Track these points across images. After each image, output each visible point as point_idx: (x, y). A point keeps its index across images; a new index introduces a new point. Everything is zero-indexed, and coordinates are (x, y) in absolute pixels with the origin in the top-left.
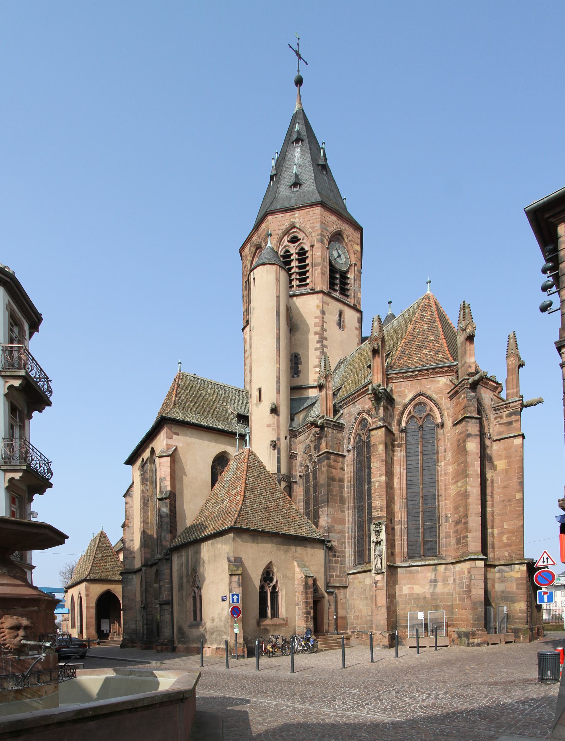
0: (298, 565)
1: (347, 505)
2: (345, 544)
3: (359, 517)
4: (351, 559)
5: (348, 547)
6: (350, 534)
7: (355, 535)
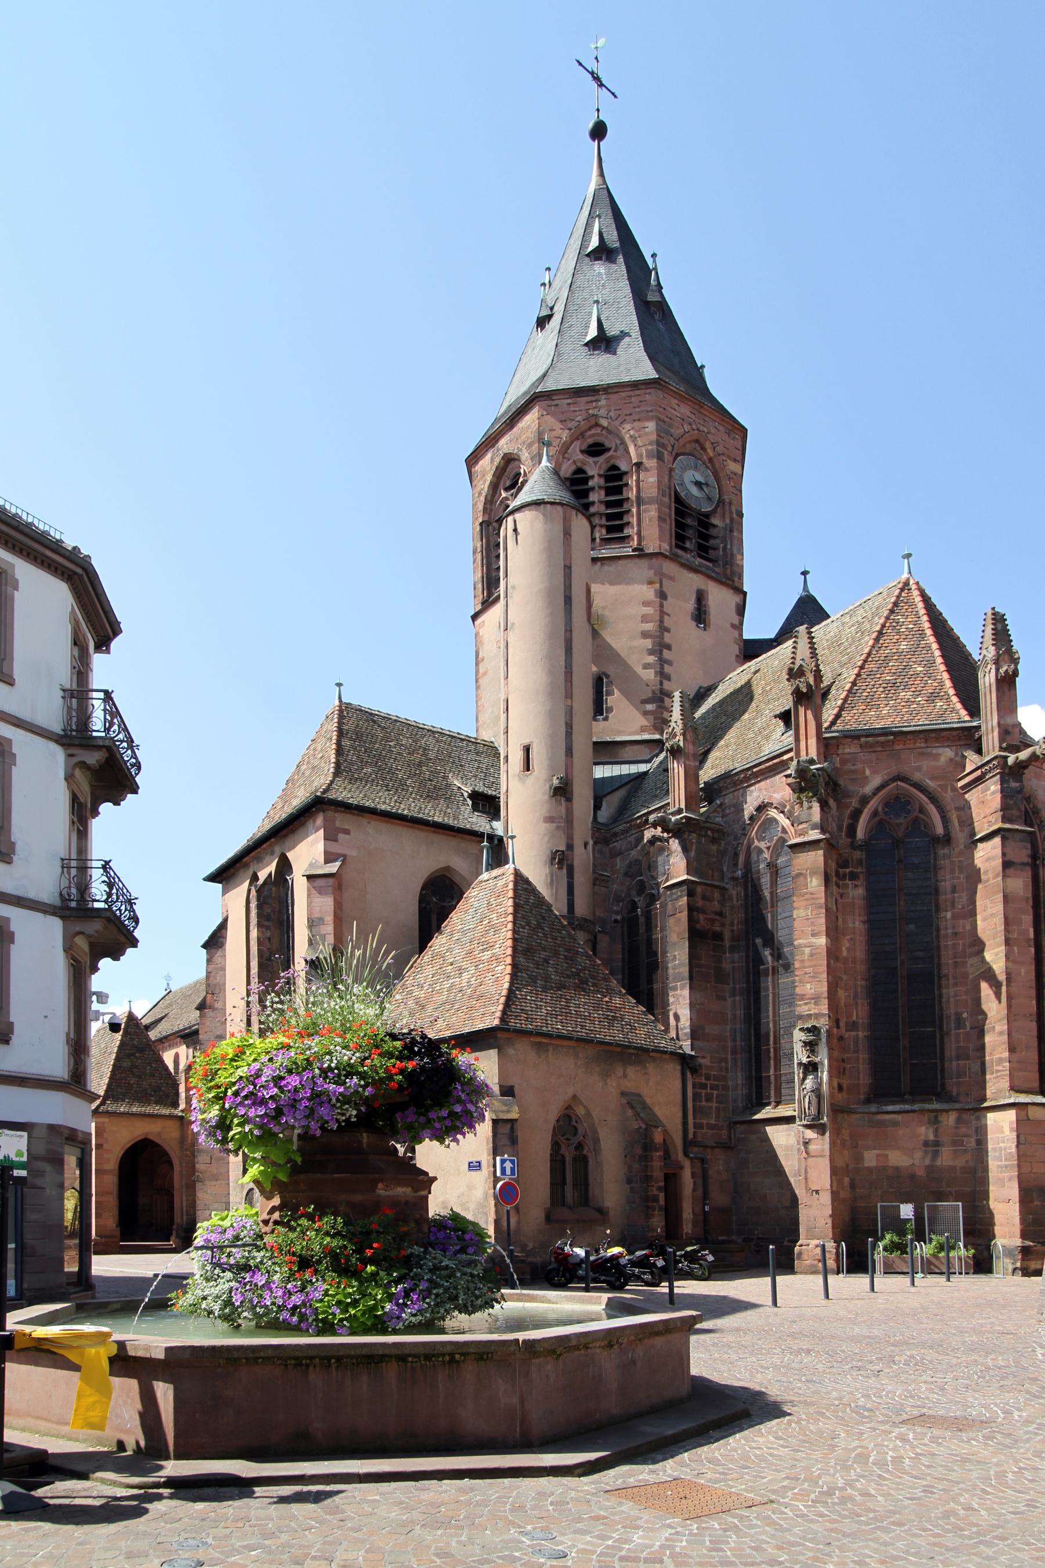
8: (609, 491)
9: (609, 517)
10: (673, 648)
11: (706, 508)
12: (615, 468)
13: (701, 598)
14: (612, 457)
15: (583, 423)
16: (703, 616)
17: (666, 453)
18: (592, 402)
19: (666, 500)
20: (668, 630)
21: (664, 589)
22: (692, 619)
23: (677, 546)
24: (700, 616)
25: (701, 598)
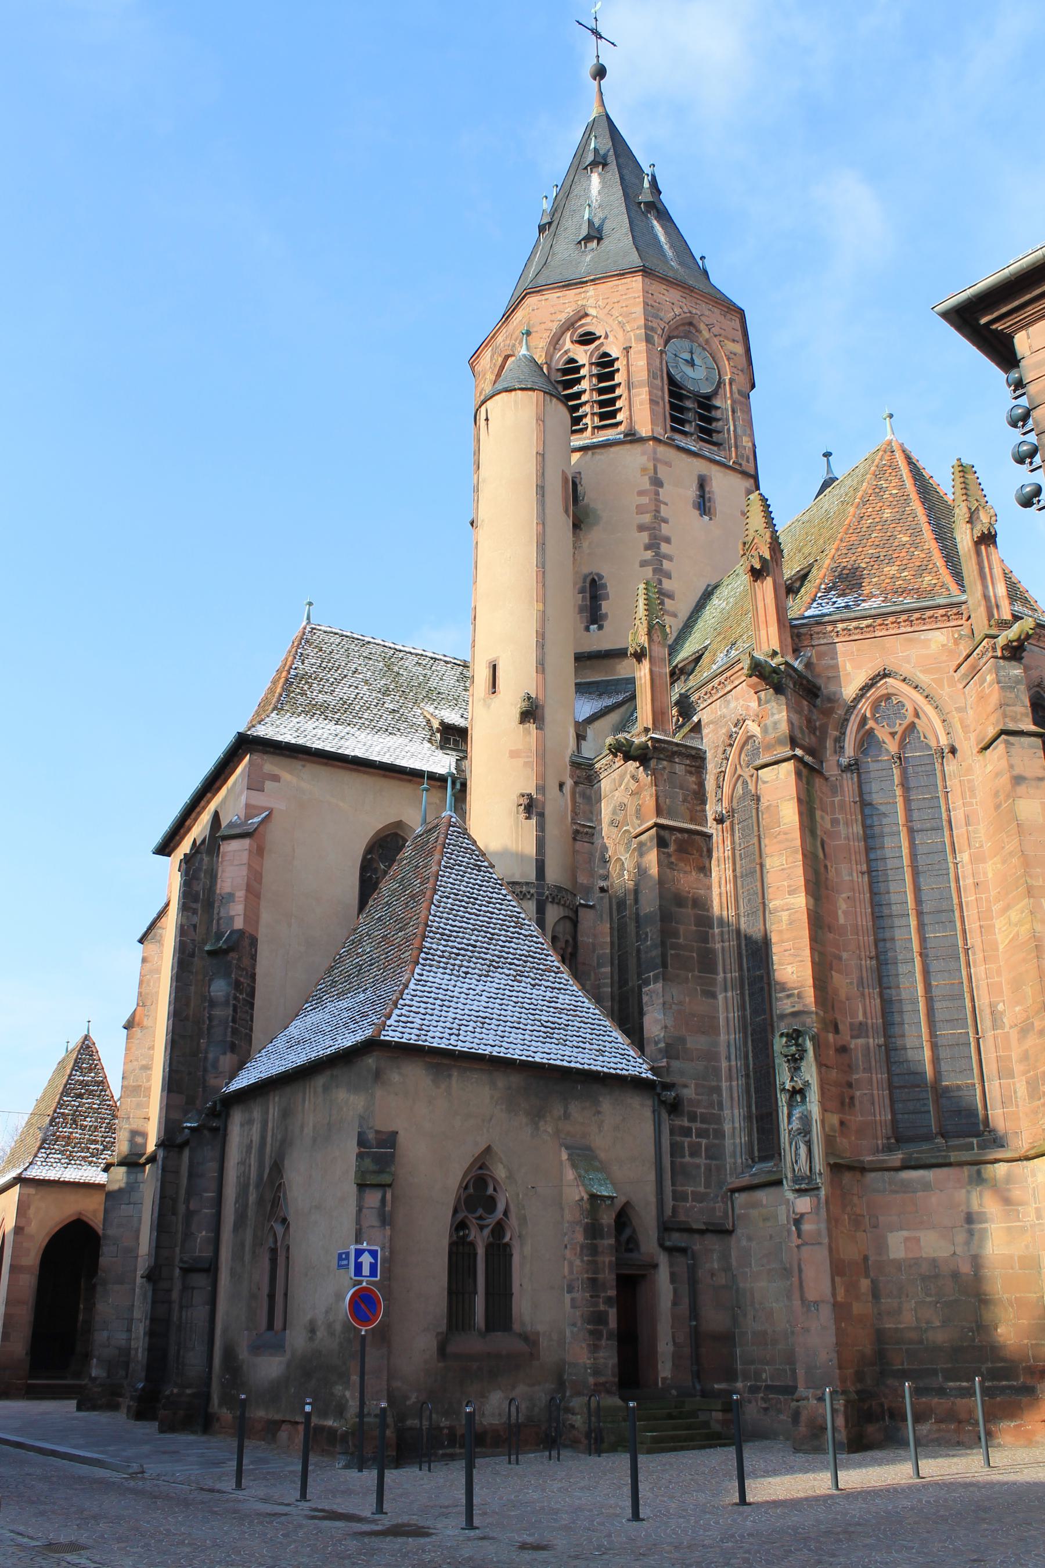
0: (570, 1158)
1: (721, 975)
2: (720, 1095)
3: (755, 1012)
4: (738, 1141)
5: (729, 1103)
6: (733, 1063)
7: (747, 1066)
8: (601, 378)
9: (602, 404)
10: (673, 540)
11: (706, 389)
12: (606, 355)
13: (702, 484)
14: (602, 344)
15: (572, 314)
16: (708, 504)
17: (656, 337)
18: (580, 293)
19: (658, 382)
20: (665, 521)
21: (659, 476)
22: (694, 507)
23: (673, 429)
24: (704, 504)
25: (702, 484)
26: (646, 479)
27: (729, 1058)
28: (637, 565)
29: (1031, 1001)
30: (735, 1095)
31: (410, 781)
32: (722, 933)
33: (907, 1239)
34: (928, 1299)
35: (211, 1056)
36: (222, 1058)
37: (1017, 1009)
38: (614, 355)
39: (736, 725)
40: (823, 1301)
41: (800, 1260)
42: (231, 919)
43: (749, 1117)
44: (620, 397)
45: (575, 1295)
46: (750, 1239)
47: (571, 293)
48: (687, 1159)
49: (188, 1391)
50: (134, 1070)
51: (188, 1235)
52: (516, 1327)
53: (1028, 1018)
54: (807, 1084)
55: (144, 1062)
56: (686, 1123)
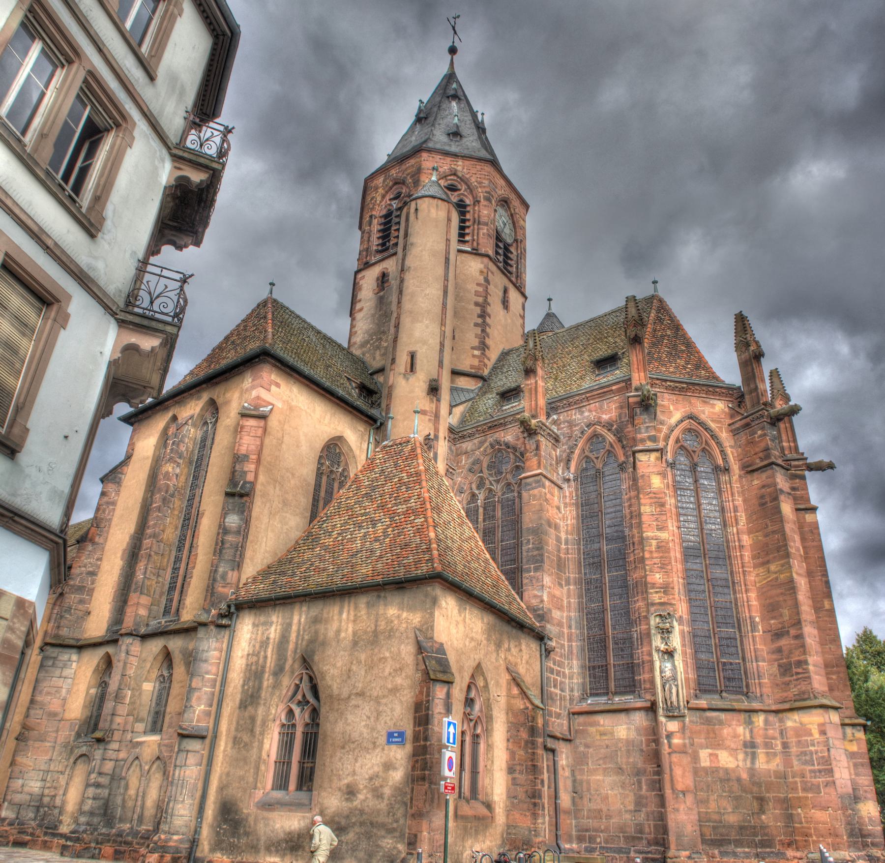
12: (461, 201)
13: (506, 291)
25: (506, 291)
26: (482, 278)
27: (570, 627)
28: (472, 325)
29: (787, 618)
30: (575, 651)
31: (351, 412)
32: (568, 549)
33: (711, 755)
34: (724, 794)
35: (221, 570)
36: (230, 573)
37: (772, 622)
38: (468, 202)
39: (587, 427)
40: (688, 791)
41: (670, 763)
42: (245, 473)
43: (583, 667)
44: (468, 227)
45: (517, 775)
46: (587, 746)
47: (449, 159)
48: (552, 689)
49: (175, 837)
50: (82, 574)
51: (186, 707)
52: (480, 797)
53: (783, 627)
54: (675, 649)
55: (91, 569)
56: (552, 666)
